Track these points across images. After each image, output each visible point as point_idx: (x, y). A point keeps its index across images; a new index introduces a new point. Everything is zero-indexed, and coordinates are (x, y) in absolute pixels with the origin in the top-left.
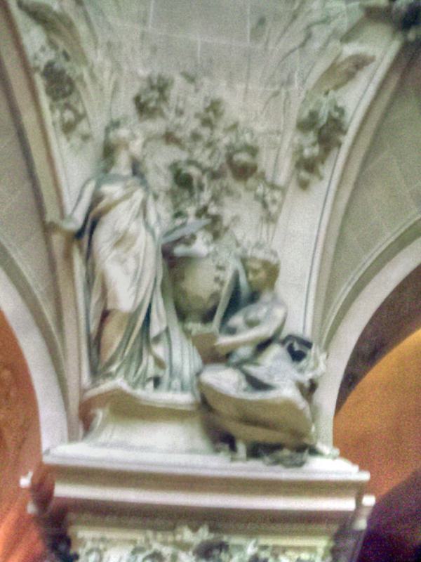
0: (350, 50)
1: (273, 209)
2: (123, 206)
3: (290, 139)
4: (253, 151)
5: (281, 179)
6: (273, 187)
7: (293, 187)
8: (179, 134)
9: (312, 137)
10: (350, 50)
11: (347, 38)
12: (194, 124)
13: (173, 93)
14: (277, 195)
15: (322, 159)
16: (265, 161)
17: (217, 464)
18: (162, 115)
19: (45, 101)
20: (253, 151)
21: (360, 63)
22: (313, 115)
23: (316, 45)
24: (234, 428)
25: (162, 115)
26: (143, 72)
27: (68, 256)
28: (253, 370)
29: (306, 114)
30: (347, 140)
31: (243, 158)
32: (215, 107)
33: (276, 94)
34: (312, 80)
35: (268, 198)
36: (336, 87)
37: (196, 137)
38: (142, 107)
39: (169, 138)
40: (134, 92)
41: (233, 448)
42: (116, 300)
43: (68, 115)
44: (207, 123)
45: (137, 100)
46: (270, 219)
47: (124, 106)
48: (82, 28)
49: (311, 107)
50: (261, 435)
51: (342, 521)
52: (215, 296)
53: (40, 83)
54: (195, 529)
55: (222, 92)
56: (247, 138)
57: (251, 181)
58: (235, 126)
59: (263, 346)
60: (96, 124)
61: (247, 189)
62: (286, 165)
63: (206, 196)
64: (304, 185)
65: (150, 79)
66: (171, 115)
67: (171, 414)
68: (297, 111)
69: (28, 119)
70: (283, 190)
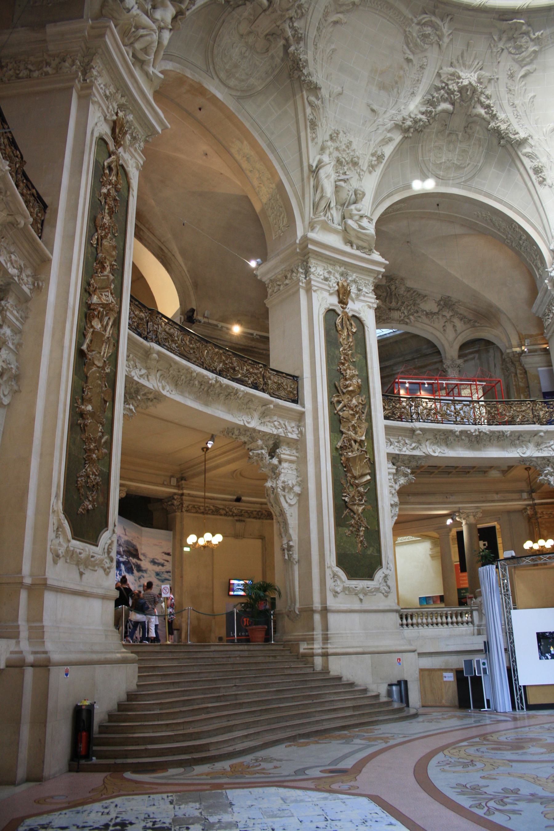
0: (389, 135)
1: (362, 177)
2: (329, 166)
3: (368, 157)
4: (358, 158)
5: (365, 169)
6: (363, 170)
7: (367, 173)
8: (340, 149)
9: (375, 159)
10: (389, 135)
11: (389, 131)
12: (344, 147)
13: (340, 136)
14: (363, 173)
15: (376, 165)
16: (361, 162)
17: (348, 249)
18: (336, 142)
19: (309, 130)
20: (358, 158)
21: (391, 140)
22: (376, 152)
23: (380, 131)
24: (353, 239)
25: (336, 142)
26: (333, 128)
27: (309, 178)
28: (360, 223)
29: (374, 151)
30: (384, 162)
31: (356, 159)
32: (350, 143)
33: (366, 143)
34: (377, 142)
35: (361, 173)
36: (383, 145)
37: (344, 150)
38: (331, 138)
39: (337, 149)
40: (330, 133)
41: (352, 246)
42: (326, 193)
43: (314, 135)
44: (347, 147)
45: (331, 135)
46: (361, 180)
47: (328, 138)
48: (321, 110)
49: (376, 149)
50: (361, 243)
51: (379, 272)
52: (346, 199)
53: (308, 124)
54: (340, 267)
55: (352, 139)
56: (357, 153)
57: (356, 168)
58: (354, 150)
59: (361, 217)
60: (320, 141)
61: (355, 170)
62: (366, 165)
63: (346, 168)
64: (370, 172)
65: (334, 130)
66: (338, 142)
67: (335, 231)
68: (371, 150)
69: (303, 134)
70: (365, 172)
